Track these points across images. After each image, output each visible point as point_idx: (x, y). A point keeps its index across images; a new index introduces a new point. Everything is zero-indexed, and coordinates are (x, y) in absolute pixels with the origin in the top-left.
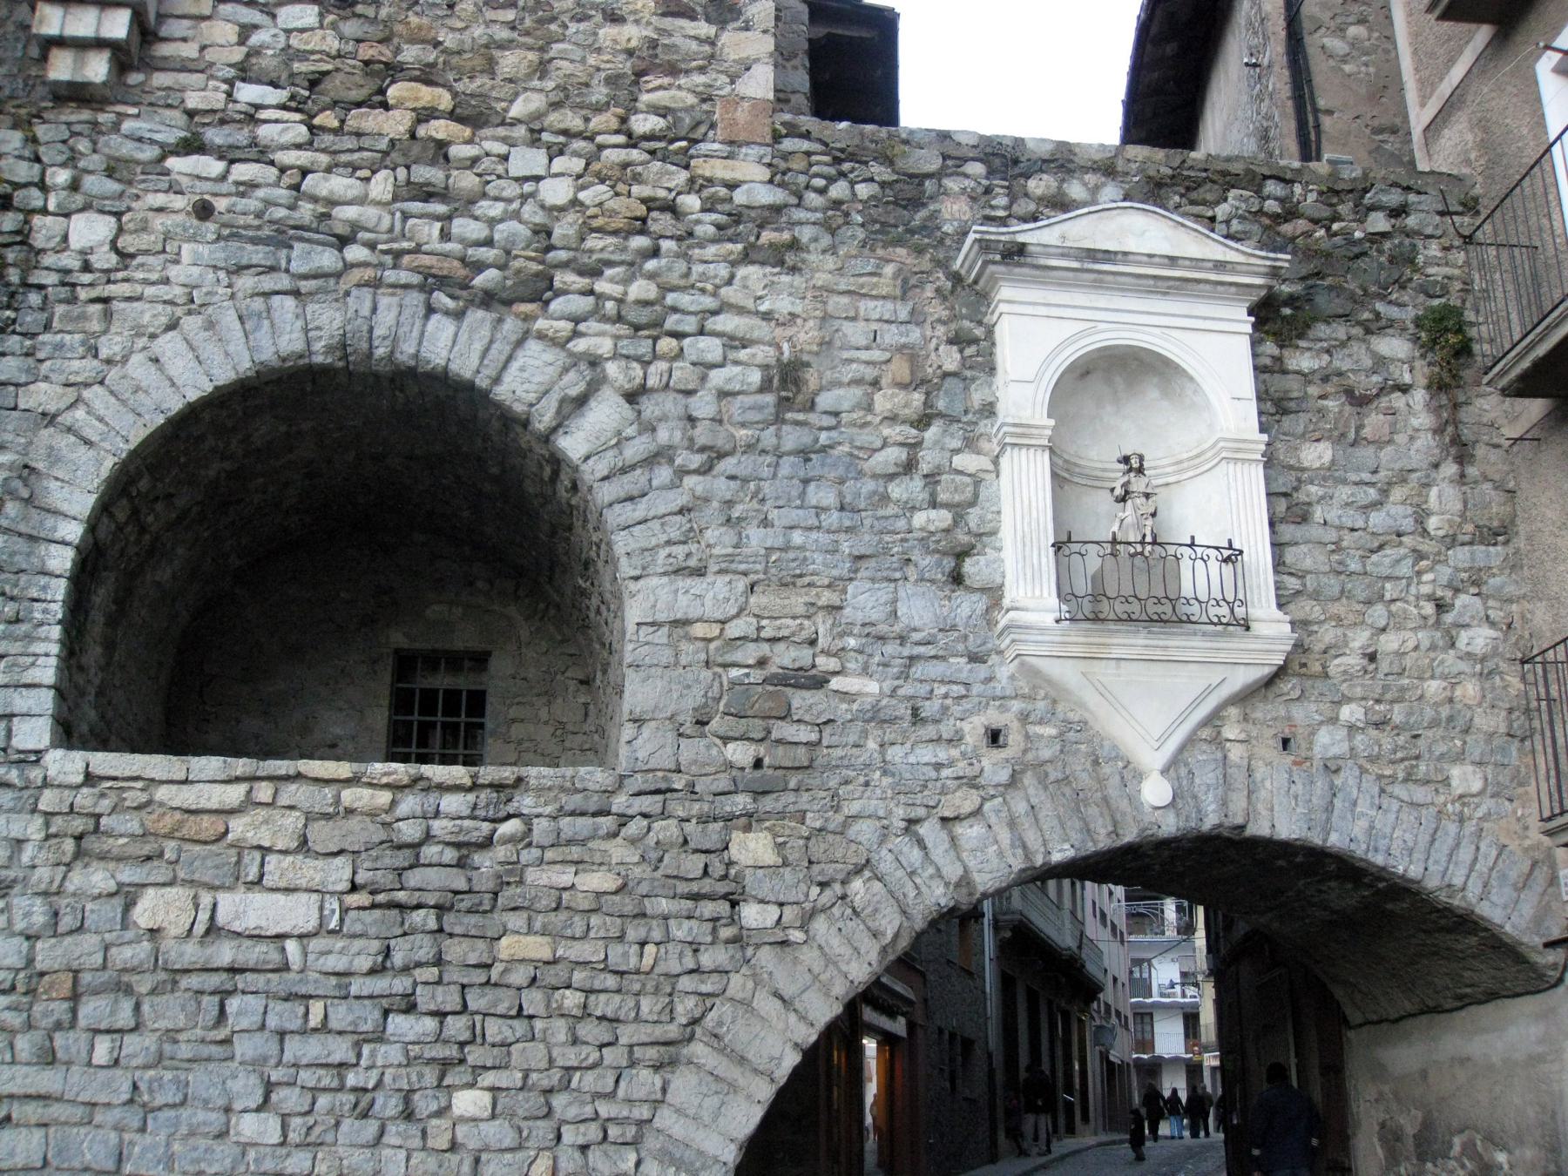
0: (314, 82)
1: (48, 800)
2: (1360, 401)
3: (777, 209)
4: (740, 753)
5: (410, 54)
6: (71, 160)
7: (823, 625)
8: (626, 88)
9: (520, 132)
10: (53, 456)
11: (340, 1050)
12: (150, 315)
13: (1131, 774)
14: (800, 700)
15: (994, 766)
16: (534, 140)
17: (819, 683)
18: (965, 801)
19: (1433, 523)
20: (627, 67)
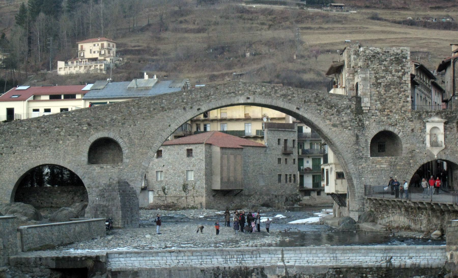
0: (380, 110)
2: (451, 128)
3: (412, 118)
4: (410, 155)
5: (386, 107)
6: (365, 117)
7: (415, 147)
8: (401, 108)
10: (368, 139)
11: (388, 174)
12: (372, 128)
13: (434, 156)
14: (414, 152)
15: (426, 155)
17: (415, 150)
18: (424, 158)
19: (456, 137)
20: (401, 107)
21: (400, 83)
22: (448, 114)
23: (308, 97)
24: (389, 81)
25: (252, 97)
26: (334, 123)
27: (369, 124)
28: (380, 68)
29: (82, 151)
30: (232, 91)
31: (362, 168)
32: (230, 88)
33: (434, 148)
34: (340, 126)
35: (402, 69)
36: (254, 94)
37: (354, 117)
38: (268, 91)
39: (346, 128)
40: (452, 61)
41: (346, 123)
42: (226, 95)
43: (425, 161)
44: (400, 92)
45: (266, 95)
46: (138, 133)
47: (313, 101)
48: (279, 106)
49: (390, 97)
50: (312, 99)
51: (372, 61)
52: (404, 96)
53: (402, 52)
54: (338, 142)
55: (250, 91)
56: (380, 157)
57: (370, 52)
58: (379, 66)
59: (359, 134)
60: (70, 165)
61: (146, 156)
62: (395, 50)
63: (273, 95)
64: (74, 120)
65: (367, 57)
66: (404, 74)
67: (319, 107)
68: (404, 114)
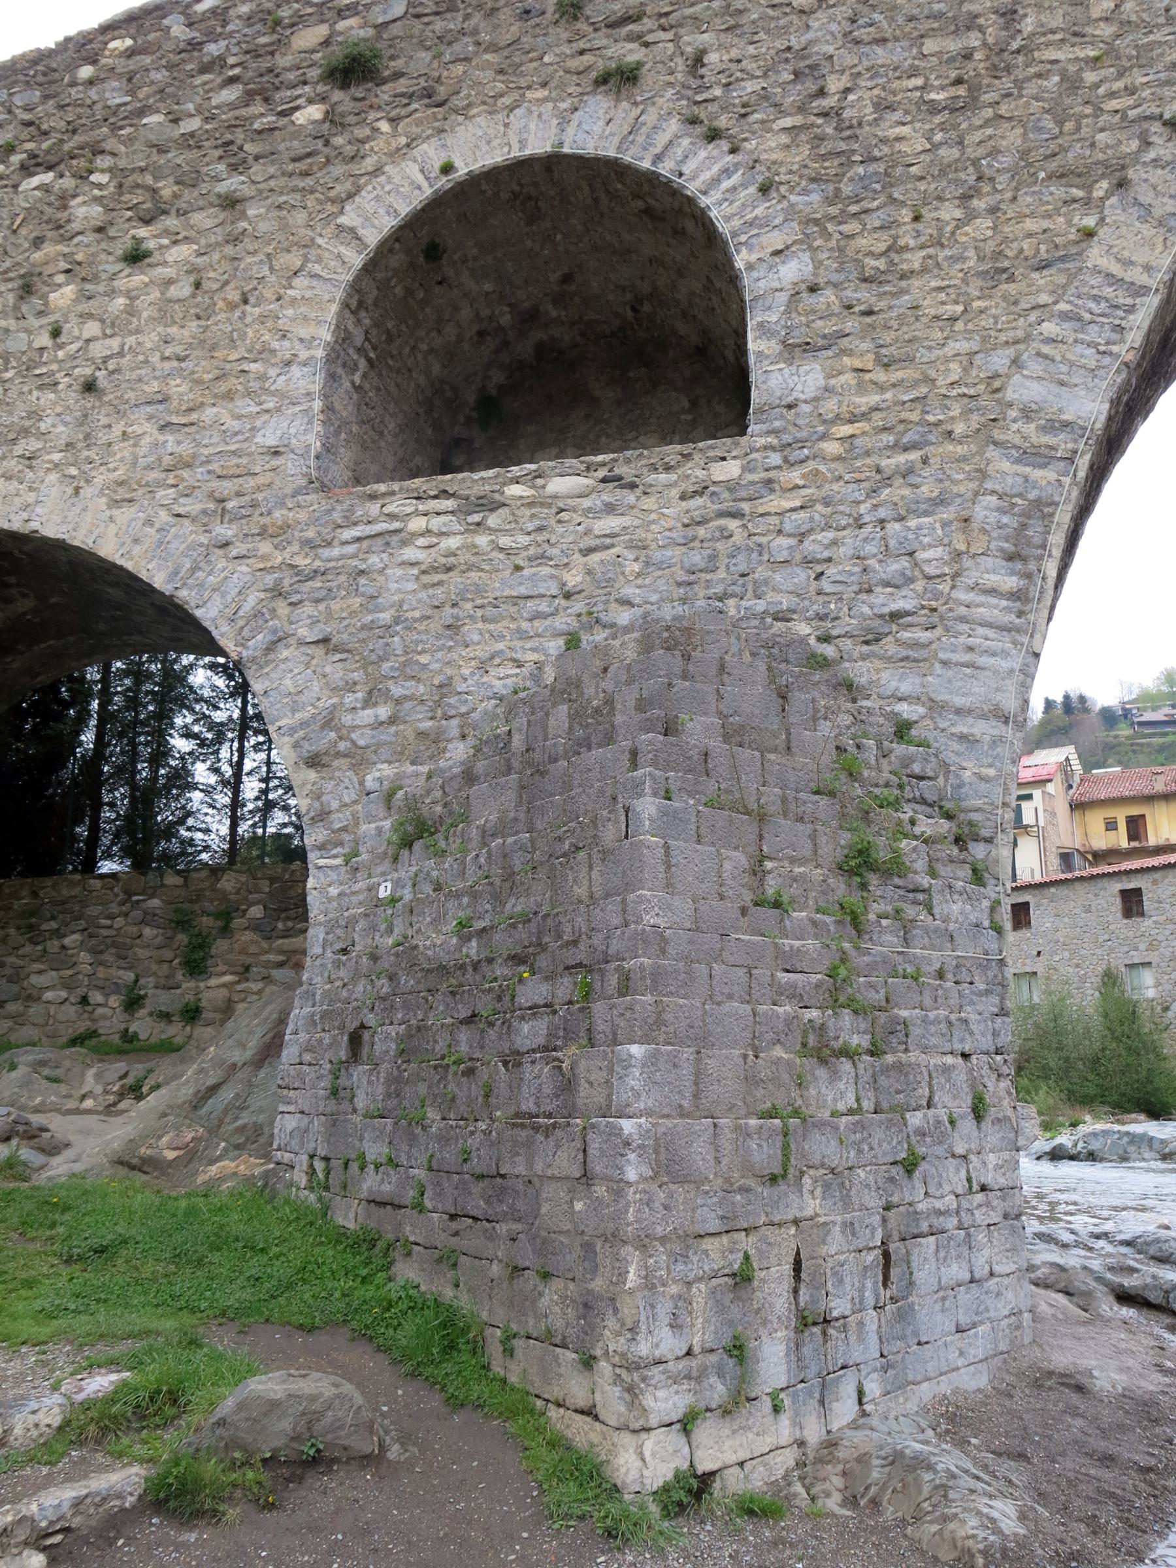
29: (264, 353)
46: (930, 46)
60: (124, 515)
61: (1059, 292)
64: (204, 69)
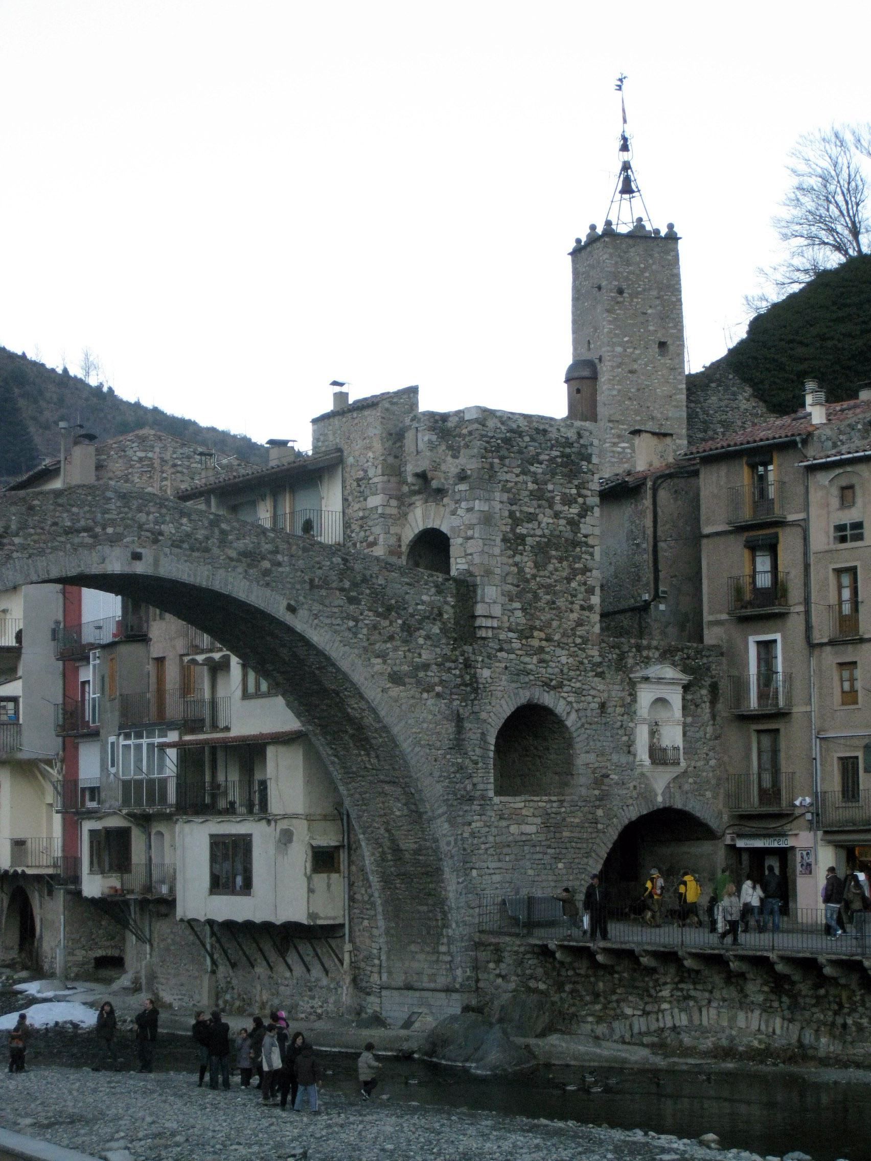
1: (495, 808)
3: (601, 663)
4: (597, 792)
5: (537, 623)
7: (608, 764)
9: (556, 644)
10: (488, 731)
11: (540, 856)
13: (656, 795)
14: (606, 780)
16: (559, 646)
18: (630, 801)
21: (575, 544)
22: (688, 658)
23: (320, 568)
24: (546, 531)
25: (147, 553)
26: (395, 669)
27: (489, 680)
28: (524, 486)
30: (83, 523)
31: (473, 835)
32: (75, 510)
33: (661, 768)
34: (413, 680)
35: (580, 495)
36: (156, 541)
37: (447, 651)
38: (200, 534)
39: (429, 689)
40: (649, 484)
41: (430, 673)
42: (62, 539)
43: (633, 813)
44: (574, 572)
45: (192, 549)
47: (334, 585)
48: (234, 595)
49: (549, 588)
50: (333, 575)
51: (502, 458)
52: (583, 589)
53: (580, 436)
54: (405, 740)
55: (140, 527)
56: (518, 799)
57: (499, 425)
58: (521, 478)
59: (466, 713)
62: (562, 429)
63: (215, 551)
65: (488, 442)
66: (585, 510)
67: (352, 607)
68: (580, 649)
